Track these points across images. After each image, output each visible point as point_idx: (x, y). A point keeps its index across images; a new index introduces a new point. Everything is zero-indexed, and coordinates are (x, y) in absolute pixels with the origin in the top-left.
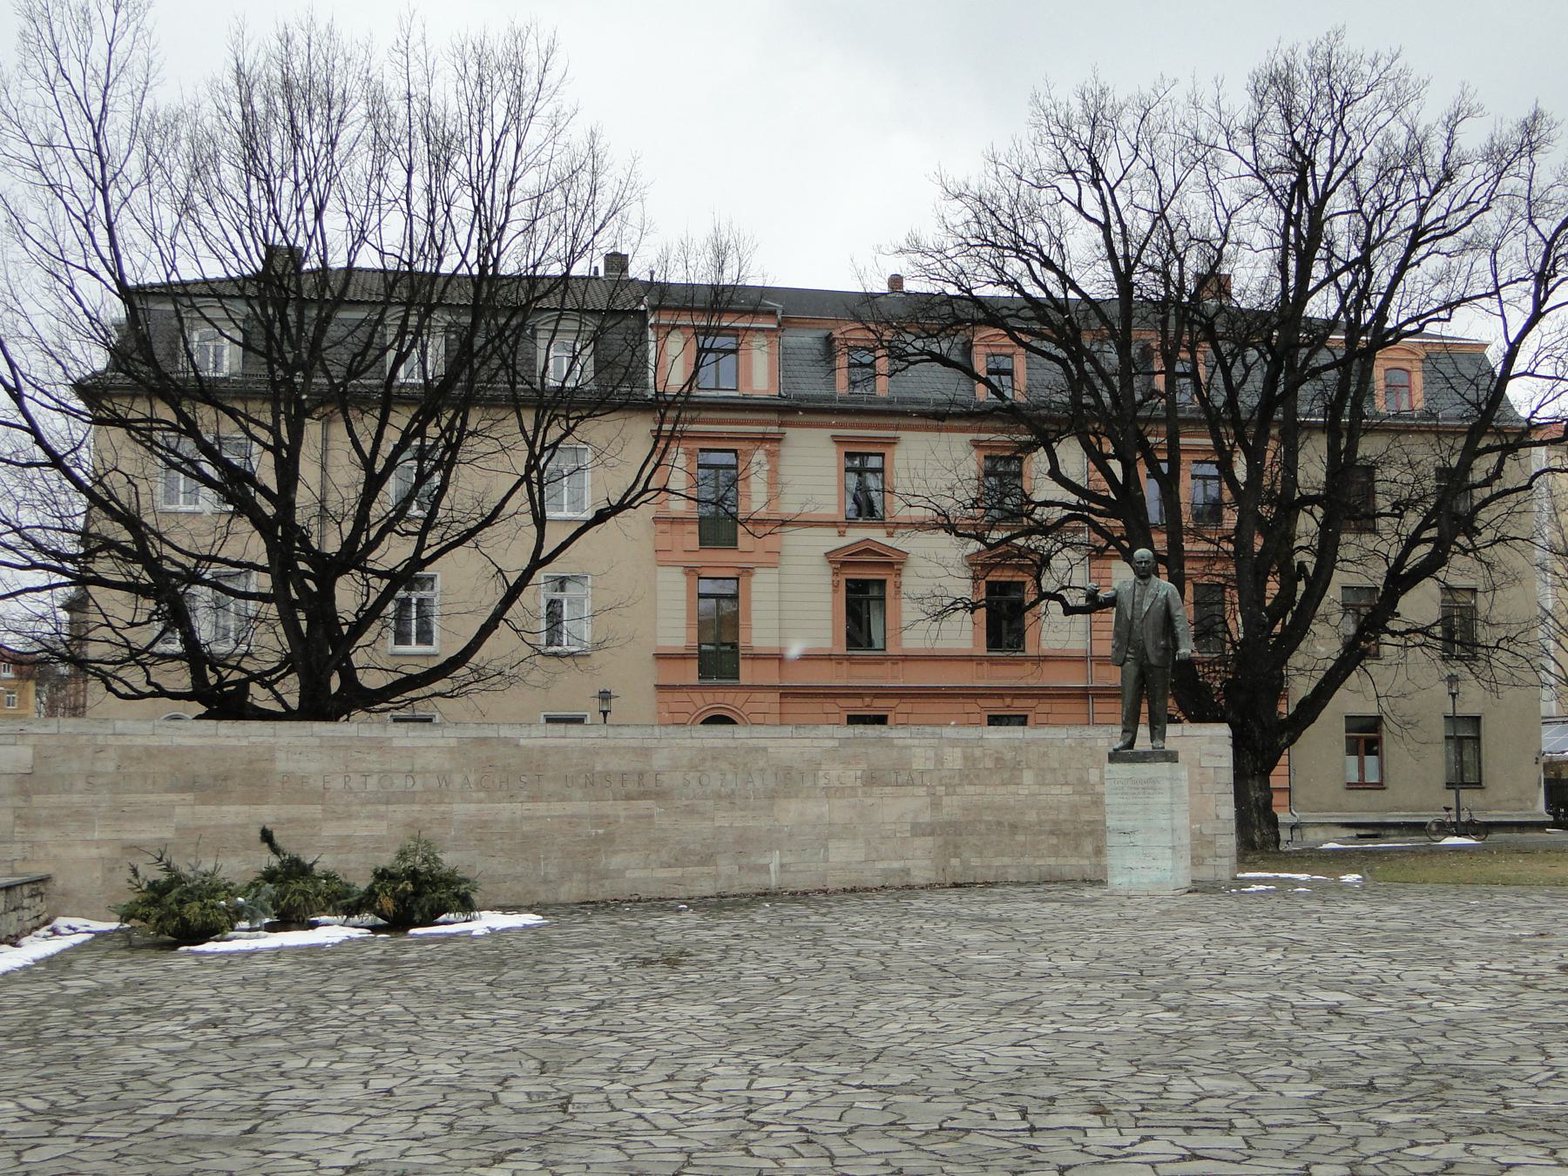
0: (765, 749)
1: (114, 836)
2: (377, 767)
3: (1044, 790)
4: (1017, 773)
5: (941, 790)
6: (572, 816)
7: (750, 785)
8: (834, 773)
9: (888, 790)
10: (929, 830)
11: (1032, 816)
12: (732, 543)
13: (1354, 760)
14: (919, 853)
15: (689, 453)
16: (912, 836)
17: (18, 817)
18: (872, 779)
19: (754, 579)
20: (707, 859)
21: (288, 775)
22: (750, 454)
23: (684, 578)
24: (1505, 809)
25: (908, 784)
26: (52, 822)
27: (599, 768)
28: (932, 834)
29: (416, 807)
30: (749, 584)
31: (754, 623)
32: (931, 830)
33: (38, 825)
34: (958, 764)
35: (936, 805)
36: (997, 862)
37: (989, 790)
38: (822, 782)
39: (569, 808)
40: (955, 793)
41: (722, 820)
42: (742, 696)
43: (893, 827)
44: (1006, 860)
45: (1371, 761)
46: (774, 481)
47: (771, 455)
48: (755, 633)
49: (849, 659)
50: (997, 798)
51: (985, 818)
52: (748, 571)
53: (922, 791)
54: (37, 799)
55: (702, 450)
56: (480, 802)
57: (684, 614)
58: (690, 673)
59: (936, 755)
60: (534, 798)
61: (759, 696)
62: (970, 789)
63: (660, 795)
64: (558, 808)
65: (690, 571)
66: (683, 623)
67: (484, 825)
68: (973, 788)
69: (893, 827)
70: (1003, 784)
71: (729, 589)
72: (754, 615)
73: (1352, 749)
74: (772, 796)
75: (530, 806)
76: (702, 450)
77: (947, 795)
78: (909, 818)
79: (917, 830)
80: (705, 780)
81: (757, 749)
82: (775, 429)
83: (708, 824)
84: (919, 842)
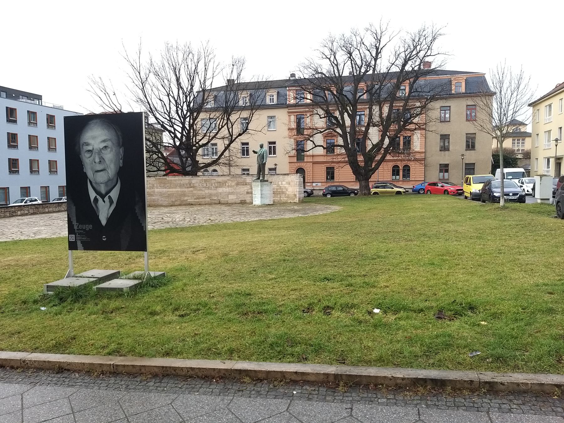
0: (215, 179)
9: (242, 186)
15: (294, 115)
18: (237, 184)
20: (204, 198)
38: (227, 185)
39: (176, 190)
41: (207, 192)
42: (305, 164)
45: (446, 174)
49: (326, 155)
55: (297, 115)
56: (160, 189)
58: (295, 160)
60: (170, 188)
61: (308, 164)
63: (193, 187)
64: (174, 190)
67: (161, 192)
73: (441, 171)
74: (217, 187)
78: (246, 191)
80: (203, 185)
83: (204, 192)
84: (248, 195)
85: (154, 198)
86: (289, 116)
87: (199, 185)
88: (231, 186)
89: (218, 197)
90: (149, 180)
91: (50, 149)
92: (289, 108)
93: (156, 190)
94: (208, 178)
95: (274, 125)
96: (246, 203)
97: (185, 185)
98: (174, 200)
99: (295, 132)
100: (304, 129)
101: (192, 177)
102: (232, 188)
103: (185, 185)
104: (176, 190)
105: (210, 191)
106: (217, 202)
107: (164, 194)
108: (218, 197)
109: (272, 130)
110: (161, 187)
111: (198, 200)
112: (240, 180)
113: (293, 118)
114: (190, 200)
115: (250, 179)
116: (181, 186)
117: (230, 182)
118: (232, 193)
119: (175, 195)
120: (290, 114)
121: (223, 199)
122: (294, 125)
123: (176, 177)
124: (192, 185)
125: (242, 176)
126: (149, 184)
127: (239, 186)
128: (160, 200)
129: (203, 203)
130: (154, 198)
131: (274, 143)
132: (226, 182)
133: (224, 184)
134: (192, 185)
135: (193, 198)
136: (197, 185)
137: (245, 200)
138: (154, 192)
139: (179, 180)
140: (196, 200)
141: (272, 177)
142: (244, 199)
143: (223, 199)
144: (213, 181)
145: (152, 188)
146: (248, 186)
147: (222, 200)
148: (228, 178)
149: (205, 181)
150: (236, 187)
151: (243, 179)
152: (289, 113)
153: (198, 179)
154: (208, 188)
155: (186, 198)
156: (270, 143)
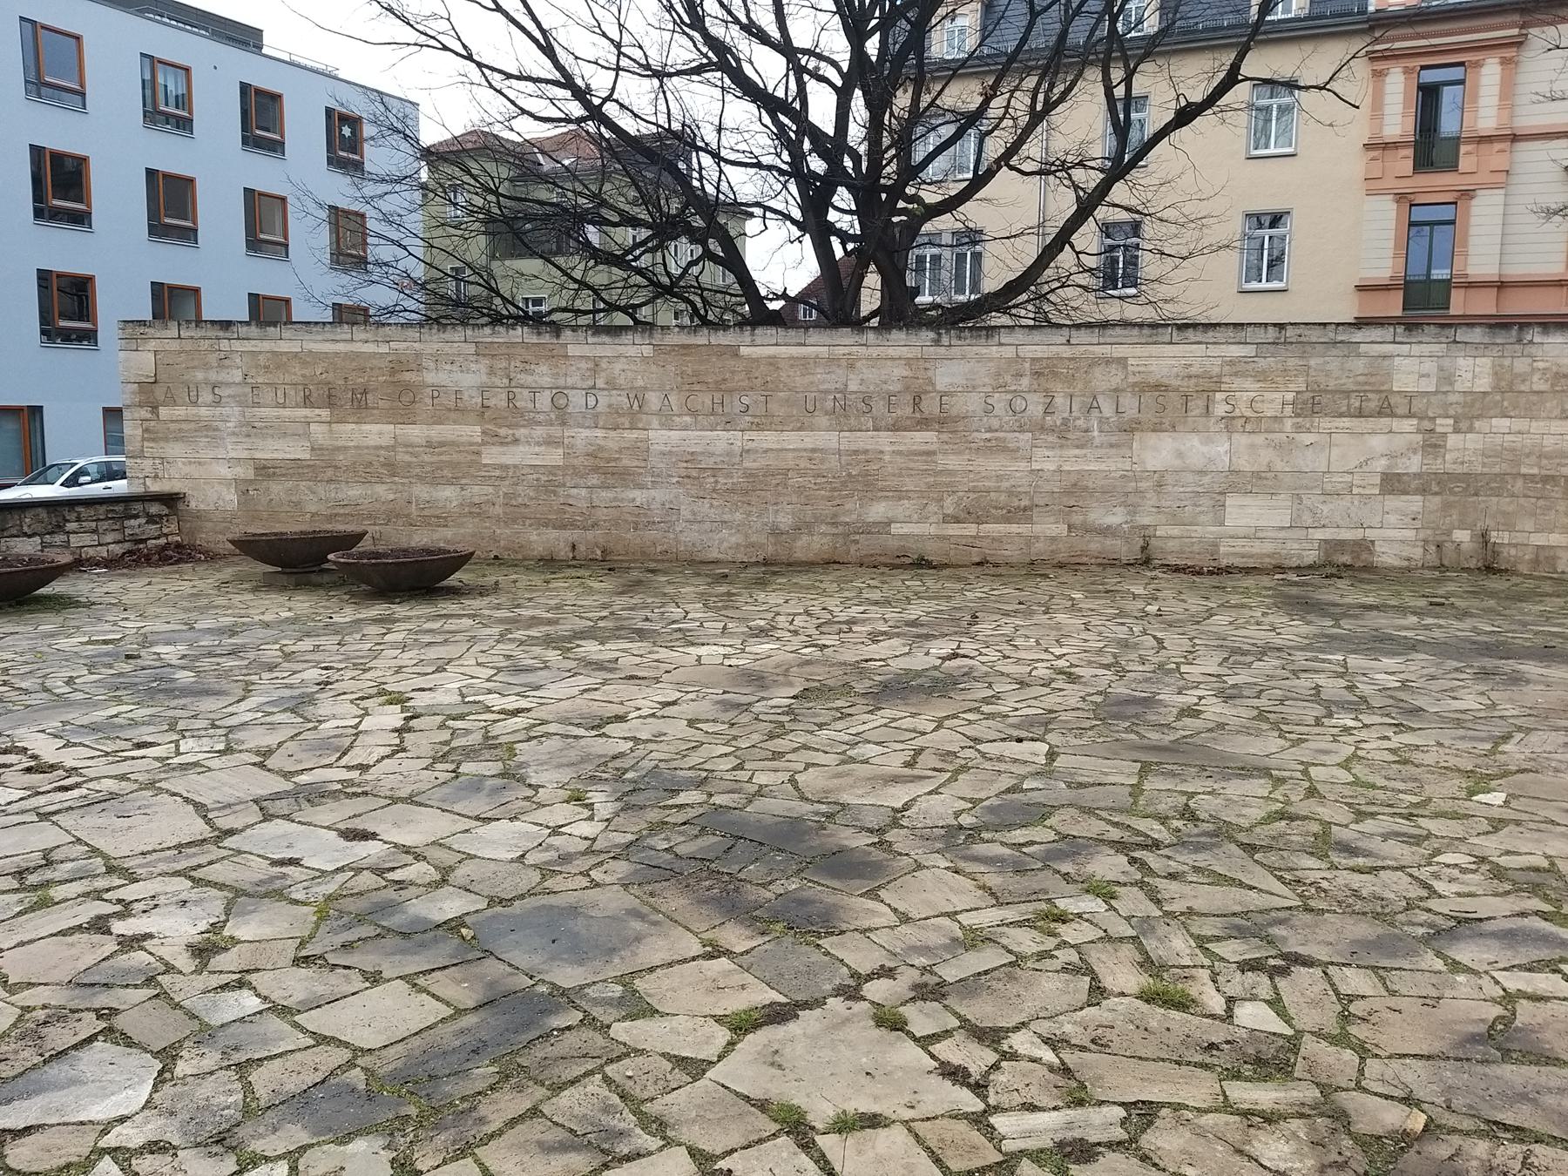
0: (1122, 362)
1: (245, 454)
2: (547, 381)
5: (1443, 425)
6: (814, 450)
7: (1095, 413)
8: (1246, 391)
9: (1346, 422)
10: (1415, 484)
12: (1453, 166)
14: (1392, 519)
15: (1407, 71)
16: (1383, 492)
17: (146, 430)
18: (1311, 406)
19: (1474, 202)
21: (436, 387)
22: (1478, 65)
25: (1380, 414)
26: (180, 437)
27: (853, 387)
28: (1423, 491)
29: (600, 433)
30: (1468, 208)
31: (1472, 250)
32: (1425, 485)
33: (166, 439)
34: (1484, 384)
35: (1433, 445)
36: (1539, 539)
37: (1536, 426)
39: (809, 440)
40: (1471, 430)
41: (1047, 460)
43: (1348, 478)
46: (1508, 91)
47: (1505, 62)
48: (1471, 260)
50: (1549, 442)
51: (1524, 470)
52: (1468, 194)
53: (1409, 425)
54: (164, 412)
55: (1423, 68)
57: (1391, 244)
59: (1441, 369)
60: (759, 427)
62: (1502, 424)
63: (943, 422)
64: (792, 440)
65: (1400, 197)
66: (1391, 253)
67: (692, 458)
68: (1506, 422)
69: (1348, 478)
71: (1445, 213)
72: (1472, 241)
74: (1131, 428)
75: (753, 435)
76: (1423, 68)
77: (1457, 431)
78: (1381, 465)
79: (1392, 483)
80: (1019, 404)
81: (1108, 361)
82: (1515, 31)
83: (1023, 465)
84: (1393, 502)
85: (639, 496)
87: (989, 410)
88: (1253, 423)
89: (1133, 509)
90: (612, 359)
91: (255, 244)
93: (661, 438)
94: (1066, 352)
95: (1285, 132)
96: (1369, 568)
97: (879, 407)
98: (785, 520)
99: (1404, 162)
100: (1456, 141)
101: (937, 342)
102: (1259, 439)
103: (879, 407)
104: (809, 440)
105: (1075, 462)
106: (1126, 550)
107: (715, 471)
108: (1133, 509)
109: (1272, 151)
110: (694, 413)
111: (971, 529)
112: (1334, 369)
113: (1398, 87)
114: (906, 529)
115: (1429, 366)
116: (845, 410)
117: (1249, 384)
118: (1257, 482)
119: (795, 480)
120: (1379, 66)
121: (1175, 531)
122: (1398, 121)
123: (815, 336)
124: (930, 406)
125: (1358, 336)
126: (612, 385)
127: (1326, 423)
128: (685, 513)
129: (1011, 552)
130: (639, 496)
131: (1276, 219)
132: (1209, 385)
133: (1197, 405)
134: (930, 406)
135: (933, 507)
136: (971, 404)
137: (1365, 546)
138: (641, 450)
139: (832, 360)
140: (953, 530)
142: (1358, 534)
143: (1175, 531)
144: (1103, 379)
145: (626, 422)
146: (1396, 424)
147: (1171, 539)
148: (1236, 351)
149: (1043, 371)
150: (1298, 429)
151: (1359, 365)
153: (980, 359)
154: (1063, 433)
155: (878, 511)
156: (1256, 219)
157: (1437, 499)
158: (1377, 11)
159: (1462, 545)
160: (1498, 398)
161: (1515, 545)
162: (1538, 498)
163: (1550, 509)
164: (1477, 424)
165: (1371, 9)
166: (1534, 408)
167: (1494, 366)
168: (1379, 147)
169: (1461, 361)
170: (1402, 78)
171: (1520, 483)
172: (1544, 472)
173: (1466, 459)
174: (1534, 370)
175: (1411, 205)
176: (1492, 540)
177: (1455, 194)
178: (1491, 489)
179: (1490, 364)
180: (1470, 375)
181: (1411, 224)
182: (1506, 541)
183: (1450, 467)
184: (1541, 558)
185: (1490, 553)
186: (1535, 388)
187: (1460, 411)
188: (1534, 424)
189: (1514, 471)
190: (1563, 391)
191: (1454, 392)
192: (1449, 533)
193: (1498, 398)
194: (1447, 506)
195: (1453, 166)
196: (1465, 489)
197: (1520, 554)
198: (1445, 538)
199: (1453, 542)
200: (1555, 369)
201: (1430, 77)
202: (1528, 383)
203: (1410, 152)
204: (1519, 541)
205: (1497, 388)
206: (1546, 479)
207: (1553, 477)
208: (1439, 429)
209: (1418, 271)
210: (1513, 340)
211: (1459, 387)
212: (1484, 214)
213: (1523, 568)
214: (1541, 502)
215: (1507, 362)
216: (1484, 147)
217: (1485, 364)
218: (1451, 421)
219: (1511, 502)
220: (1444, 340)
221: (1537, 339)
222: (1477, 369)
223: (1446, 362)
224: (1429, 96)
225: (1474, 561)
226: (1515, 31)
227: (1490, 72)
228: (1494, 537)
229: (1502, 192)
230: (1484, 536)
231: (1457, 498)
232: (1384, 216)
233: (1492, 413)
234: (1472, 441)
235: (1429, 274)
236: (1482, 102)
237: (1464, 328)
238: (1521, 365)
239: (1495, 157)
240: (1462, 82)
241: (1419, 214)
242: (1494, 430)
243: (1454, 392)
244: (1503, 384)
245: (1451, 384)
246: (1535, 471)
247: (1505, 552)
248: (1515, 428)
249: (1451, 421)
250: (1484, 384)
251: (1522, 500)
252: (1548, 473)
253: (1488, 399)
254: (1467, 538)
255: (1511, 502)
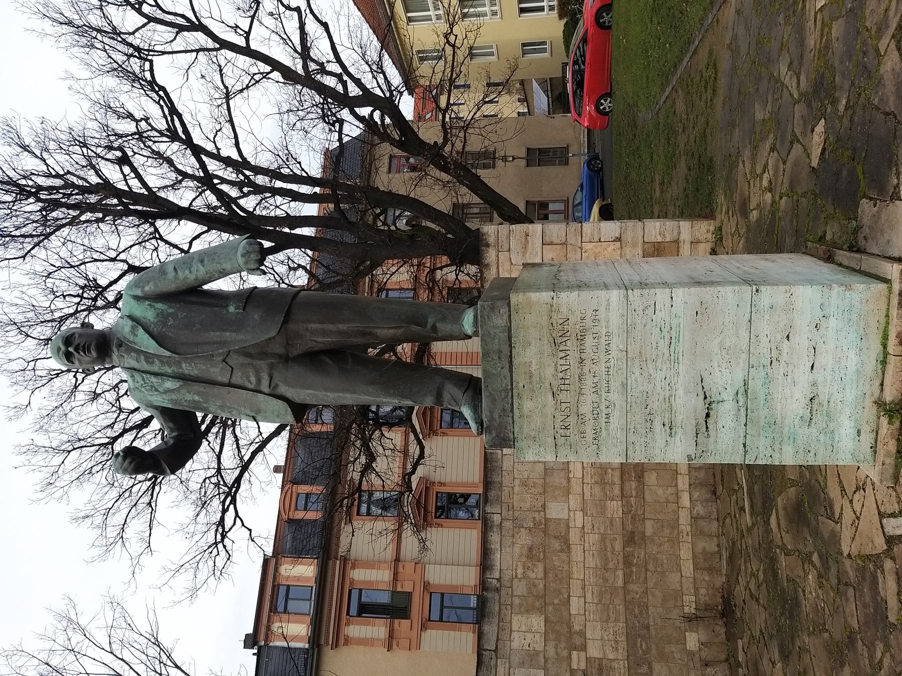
3: (576, 487)
4: (551, 528)
11: (615, 508)
12: (409, 595)
13: (551, 216)
15: (348, 624)
19: (432, 582)
22: (352, 582)
23: (429, 631)
24: (580, 135)
30: (435, 585)
31: (460, 583)
34: (537, 622)
36: (688, 568)
37: (577, 573)
40: (582, 633)
44: (685, 553)
47: (353, 568)
48: (466, 583)
50: (592, 562)
51: (620, 583)
52: (426, 586)
55: (348, 614)
59: (522, 664)
62: (576, 605)
65: (424, 627)
66: (458, 633)
70: (567, 546)
71: (436, 599)
72: (454, 583)
77: (584, 648)
82: (338, 562)
86: (347, 641)
92: (322, 642)
99: (402, 625)
100: (394, 593)
113: (355, 630)
120: (342, 641)
122: (377, 629)
141: (507, 480)
152: (336, 645)
157: (657, 667)
158: (309, 643)
159: (703, 639)
160: (550, 608)
161: (696, 589)
162: (647, 570)
163: (656, 560)
164: (577, 628)
165: (307, 646)
166: (559, 576)
167: (520, 613)
168: (390, 642)
169: (515, 644)
170: (351, 627)
171: (633, 587)
172: (621, 565)
173: (611, 637)
174: (525, 576)
175: (430, 620)
176: (693, 611)
177: (426, 593)
178: (641, 613)
179: (519, 617)
180: (529, 635)
181: (441, 620)
182: (693, 599)
183: (621, 654)
184: (707, 565)
185: (706, 614)
186: (541, 575)
187: (563, 645)
188: (575, 576)
189: (621, 592)
190: (544, 552)
191: (545, 651)
192: (691, 654)
193: (550, 608)
194: (663, 657)
195: (409, 595)
196: (643, 637)
197: (704, 584)
198: (697, 659)
199: (700, 650)
200: (524, 559)
201: (354, 610)
202: (536, 581)
203: (396, 621)
204: (691, 586)
205: (542, 610)
206: (628, 562)
207: (625, 557)
208: (583, 666)
209: (470, 616)
210: (497, 596)
211: (539, 647)
212: (438, 576)
213: (720, 581)
214: (651, 567)
215: (517, 601)
216: (400, 577)
217: (518, 622)
218: (575, 654)
219: (653, 595)
220: (493, 662)
221: (496, 575)
222: (523, 628)
223: (515, 659)
224: (367, 610)
225: (717, 628)
226: (338, 562)
227: (358, 575)
228: (690, 609)
229: (427, 566)
230: (690, 619)
231: (654, 647)
232: (434, 638)
233: (565, 614)
234: (594, 632)
235: (473, 609)
236: (374, 578)
237: (484, 641)
238: (520, 588)
239: (407, 570)
240: (361, 590)
241: (435, 616)
242: (582, 612)
243: (545, 651)
244: (537, 604)
245: (537, 653)
246: (620, 573)
247: (702, 599)
248: (579, 592)
249: (575, 654)
250: (537, 622)
251: (650, 584)
252: (621, 562)
253: (552, 618)
254: (694, 635)
255: (653, 595)
